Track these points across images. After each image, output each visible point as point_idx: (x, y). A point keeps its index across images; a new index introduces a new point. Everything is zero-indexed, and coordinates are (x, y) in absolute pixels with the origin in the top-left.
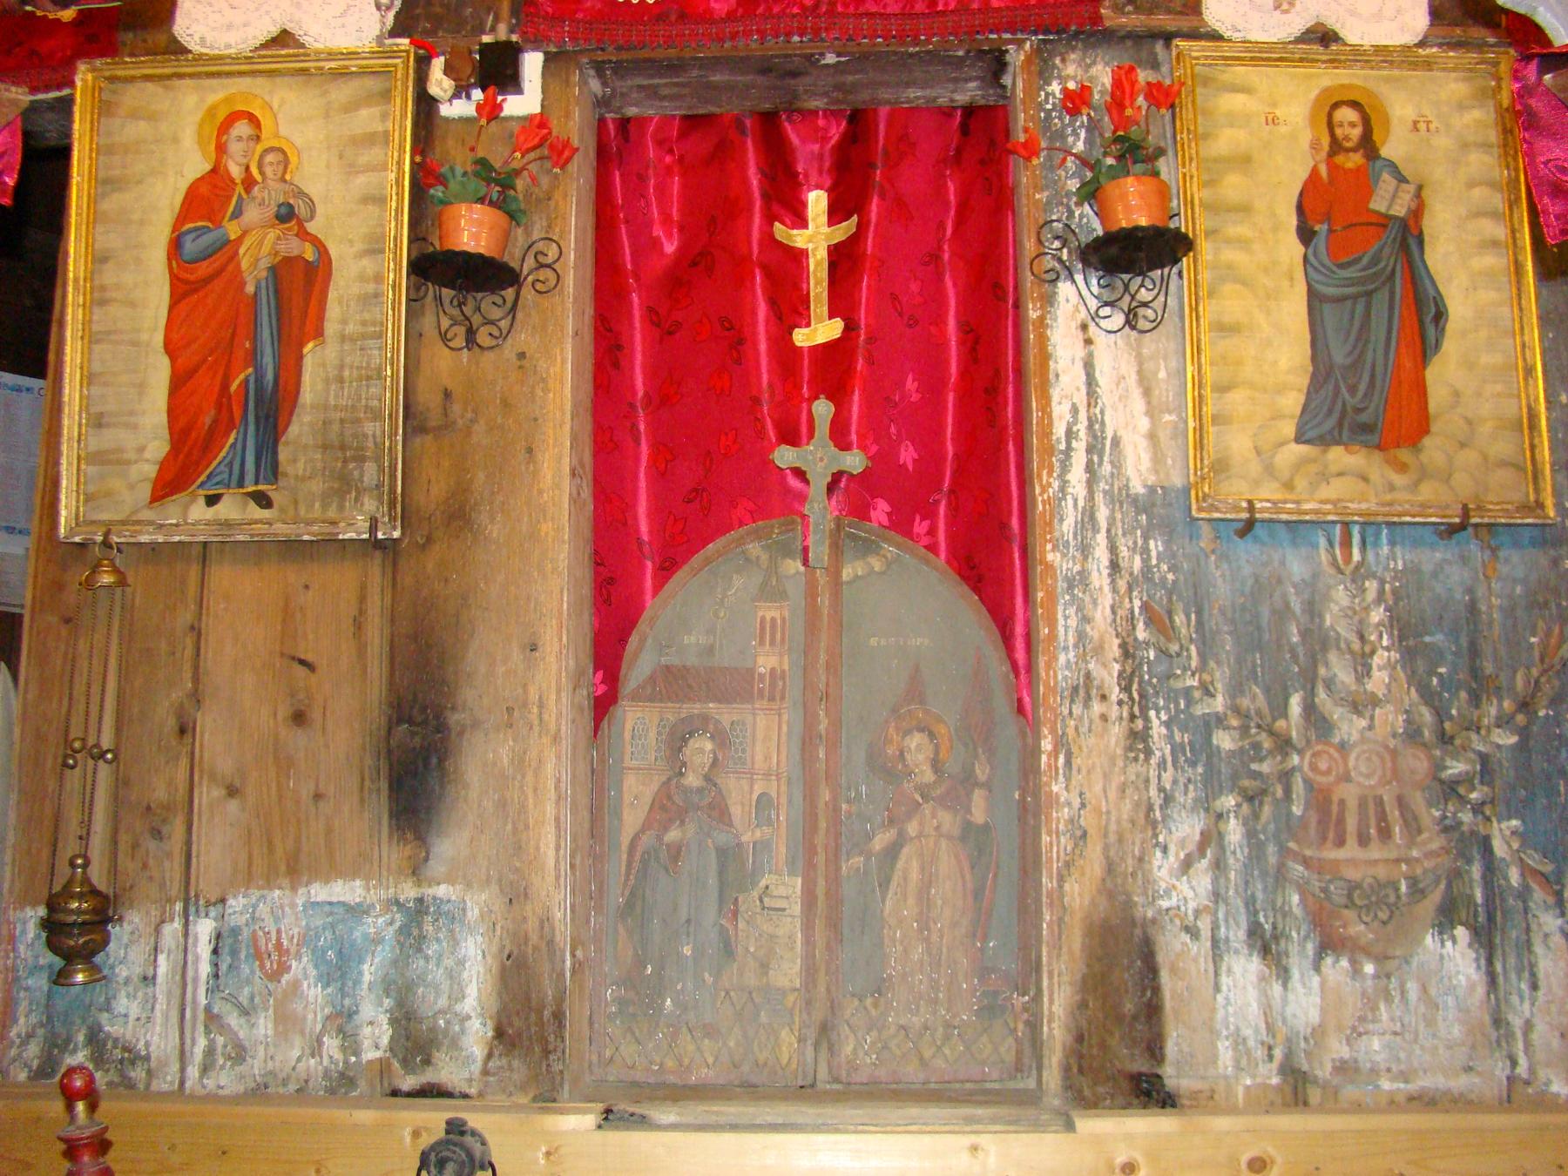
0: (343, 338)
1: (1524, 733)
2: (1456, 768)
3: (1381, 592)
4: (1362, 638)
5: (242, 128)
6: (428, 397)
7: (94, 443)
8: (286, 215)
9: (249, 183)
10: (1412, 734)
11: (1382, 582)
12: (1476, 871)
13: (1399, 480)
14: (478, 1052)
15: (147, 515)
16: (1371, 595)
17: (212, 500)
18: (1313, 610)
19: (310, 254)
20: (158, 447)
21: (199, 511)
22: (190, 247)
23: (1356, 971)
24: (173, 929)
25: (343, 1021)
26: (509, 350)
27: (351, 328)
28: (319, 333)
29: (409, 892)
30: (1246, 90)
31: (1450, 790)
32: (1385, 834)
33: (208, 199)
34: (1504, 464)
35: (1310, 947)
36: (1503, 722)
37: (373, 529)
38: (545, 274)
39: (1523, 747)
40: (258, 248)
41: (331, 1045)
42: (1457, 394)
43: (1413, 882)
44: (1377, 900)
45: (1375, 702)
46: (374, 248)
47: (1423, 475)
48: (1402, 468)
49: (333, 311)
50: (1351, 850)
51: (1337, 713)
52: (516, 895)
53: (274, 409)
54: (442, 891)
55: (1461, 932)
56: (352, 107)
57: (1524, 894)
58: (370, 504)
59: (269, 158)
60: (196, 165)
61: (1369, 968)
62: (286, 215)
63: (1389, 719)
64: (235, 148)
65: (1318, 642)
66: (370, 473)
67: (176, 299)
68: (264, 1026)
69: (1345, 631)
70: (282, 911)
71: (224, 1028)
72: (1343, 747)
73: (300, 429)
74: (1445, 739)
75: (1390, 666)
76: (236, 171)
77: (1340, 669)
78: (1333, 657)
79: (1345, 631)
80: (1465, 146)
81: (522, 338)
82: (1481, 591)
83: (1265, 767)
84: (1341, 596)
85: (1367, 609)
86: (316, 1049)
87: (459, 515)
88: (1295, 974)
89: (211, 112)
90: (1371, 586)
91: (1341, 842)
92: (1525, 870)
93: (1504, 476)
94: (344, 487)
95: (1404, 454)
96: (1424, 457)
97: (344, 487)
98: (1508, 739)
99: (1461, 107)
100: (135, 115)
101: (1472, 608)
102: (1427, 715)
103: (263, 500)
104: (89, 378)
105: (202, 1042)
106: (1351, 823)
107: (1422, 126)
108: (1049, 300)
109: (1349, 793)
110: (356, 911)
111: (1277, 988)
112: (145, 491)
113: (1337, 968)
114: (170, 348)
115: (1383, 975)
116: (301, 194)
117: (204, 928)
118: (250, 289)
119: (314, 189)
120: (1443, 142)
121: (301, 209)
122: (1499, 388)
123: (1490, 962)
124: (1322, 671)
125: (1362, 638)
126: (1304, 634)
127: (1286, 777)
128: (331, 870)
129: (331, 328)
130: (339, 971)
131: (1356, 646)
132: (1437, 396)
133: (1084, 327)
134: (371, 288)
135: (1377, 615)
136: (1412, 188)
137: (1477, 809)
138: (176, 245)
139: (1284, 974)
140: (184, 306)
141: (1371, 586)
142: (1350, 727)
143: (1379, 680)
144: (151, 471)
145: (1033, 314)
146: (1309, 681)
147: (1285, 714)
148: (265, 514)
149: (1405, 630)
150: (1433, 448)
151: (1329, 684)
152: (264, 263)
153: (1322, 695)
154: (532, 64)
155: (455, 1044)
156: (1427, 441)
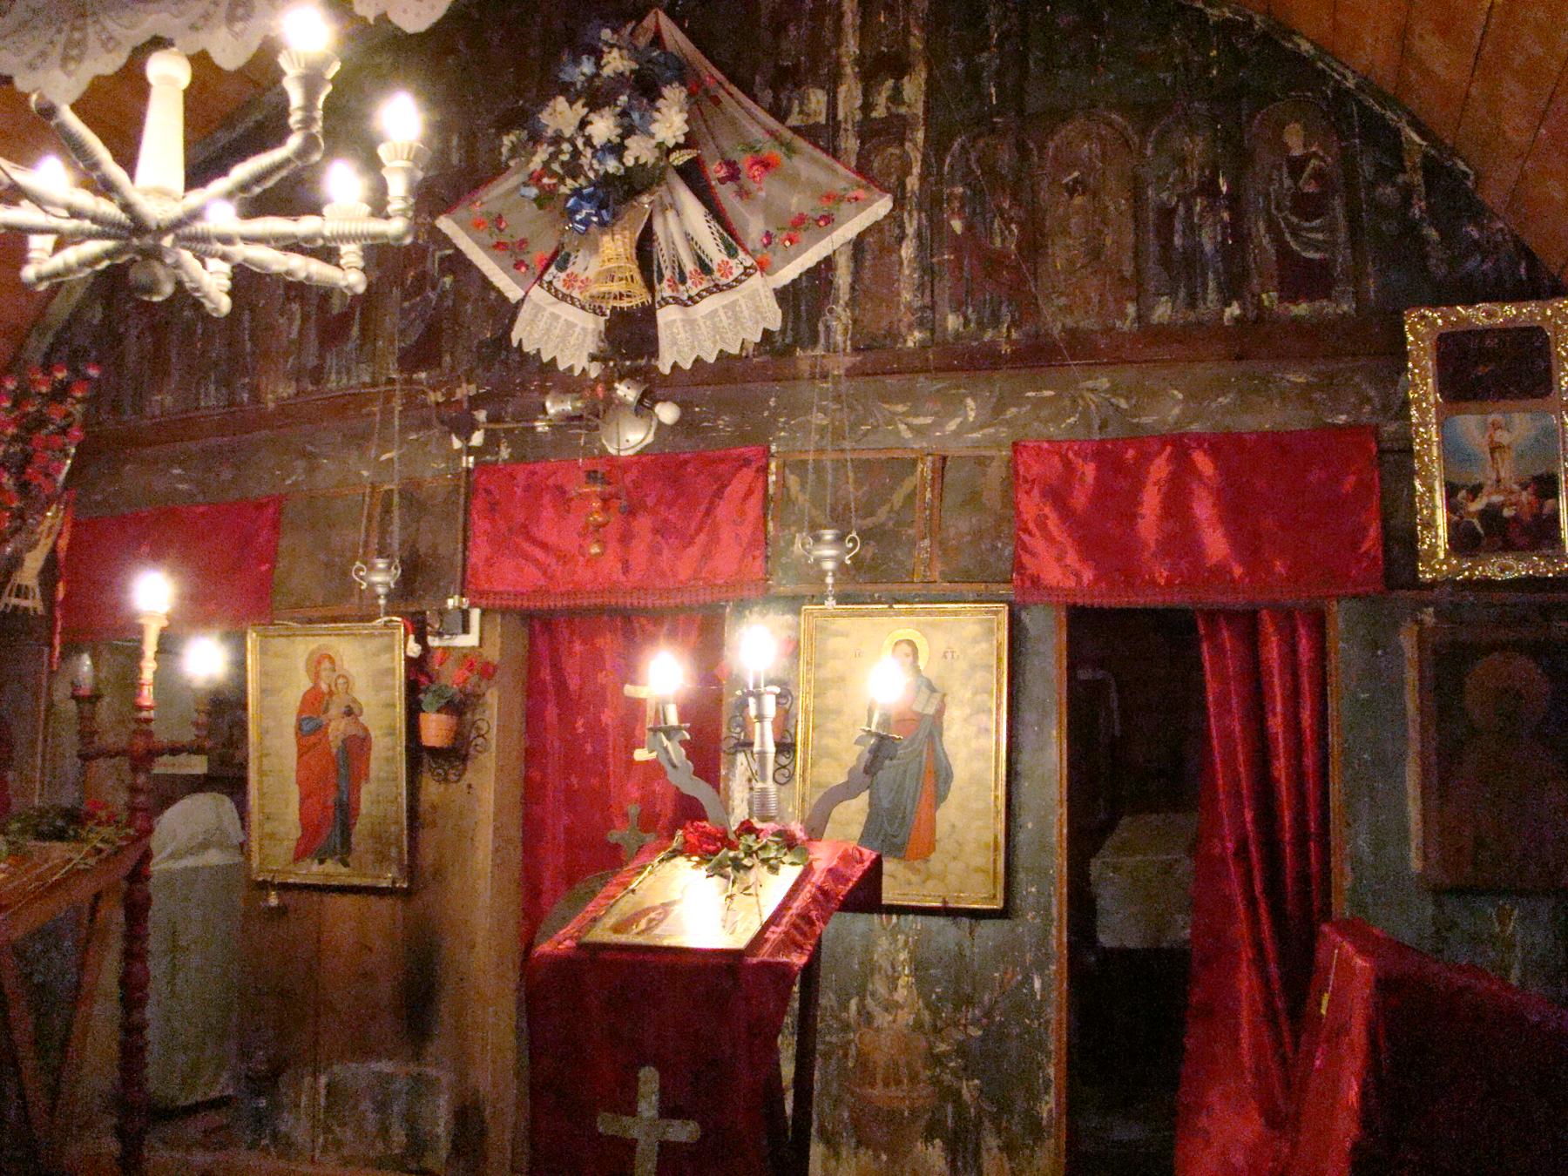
0: (378, 779)
1: (986, 1030)
2: (942, 1047)
3: (906, 942)
4: (893, 967)
5: (326, 664)
6: (424, 806)
7: (268, 828)
8: (349, 712)
9: (331, 693)
10: (918, 1026)
11: (907, 936)
12: (950, 1108)
13: (914, 879)
14: (444, 1154)
15: (291, 867)
16: (901, 944)
17: (322, 862)
18: (868, 949)
19: (361, 734)
20: (296, 833)
21: (315, 867)
22: (306, 728)
23: (877, 1157)
24: (308, 1080)
25: (384, 1131)
26: (463, 784)
27: (382, 774)
28: (367, 780)
29: (413, 1068)
30: (845, 635)
31: (937, 1060)
32: (899, 1082)
33: (315, 702)
34: (978, 870)
35: (853, 1141)
36: (976, 1022)
37: (394, 882)
38: (480, 741)
39: (983, 1039)
40: (337, 729)
41: (380, 1146)
42: (953, 826)
43: (913, 1111)
44: (891, 1117)
45: (898, 1006)
46: (391, 732)
47: (929, 877)
48: (916, 871)
49: (373, 765)
50: (877, 1092)
51: (877, 1011)
52: (462, 1076)
53: (346, 813)
54: (432, 1072)
55: (937, 1141)
56: (377, 654)
57: (978, 1125)
58: (394, 868)
59: (341, 681)
60: (305, 684)
61: (884, 1157)
62: (349, 712)
63: (905, 1018)
64: (323, 674)
65: (869, 968)
66: (394, 852)
67: (300, 755)
68: (348, 1135)
69: (886, 965)
70: (358, 1073)
71: (332, 1132)
72: (878, 1030)
73: (361, 827)
74: (936, 1030)
75: (908, 986)
76: (324, 687)
77: (879, 986)
78: (877, 977)
79: (886, 965)
80: (974, 667)
81: (469, 776)
82: (967, 943)
83: (834, 1039)
84: (884, 943)
85: (898, 951)
86: (372, 1145)
87: (438, 872)
88: (844, 1154)
89: (312, 653)
90: (901, 938)
91: (873, 1085)
92: (980, 1110)
93: (979, 877)
94: (382, 858)
95: (917, 864)
96: (930, 865)
97: (382, 858)
98: (976, 1032)
99: (975, 641)
100: (276, 655)
101: (961, 955)
102: (926, 1016)
103: (346, 865)
104: (262, 795)
105: (321, 1140)
106: (879, 1077)
107: (949, 655)
108: (732, 764)
109: (880, 1059)
110: (390, 1078)
111: (833, 1163)
112: (290, 856)
113: (866, 1156)
114: (299, 783)
115: (892, 1161)
116: (355, 701)
117: (323, 1080)
118: (334, 751)
119: (362, 699)
120: (962, 665)
121: (356, 710)
122: (980, 823)
123: (954, 1161)
124: (870, 986)
125: (893, 967)
126: (861, 963)
127: (845, 1045)
128: (379, 1058)
129: (372, 774)
130: (382, 1107)
131: (890, 972)
132: (942, 828)
133: (750, 780)
134: (390, 753)
135: (903, 956)
136: (938, 696)
137: (954, 1073)
138: (299, 728)
139: (837, 1155)
140: (306, 757)
141: (901, 938)
142: (882, 1019)
143: (901, 994)
144: (293, 844)
145: (723, 772)
146: (862, 993)
147: (846, 1009)
148: (344, 870)
149: (919, 967)
150: (936, 861)
151: (873, 994)
152: (341, 737)
153: (869, 1000)
154: (475, 614)
155: (434, 1150)
156: (933, 856)
